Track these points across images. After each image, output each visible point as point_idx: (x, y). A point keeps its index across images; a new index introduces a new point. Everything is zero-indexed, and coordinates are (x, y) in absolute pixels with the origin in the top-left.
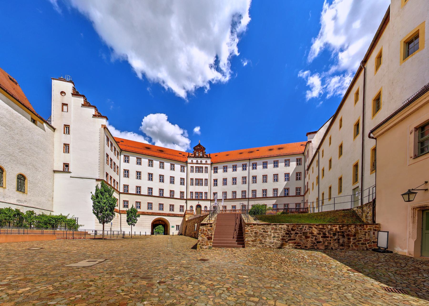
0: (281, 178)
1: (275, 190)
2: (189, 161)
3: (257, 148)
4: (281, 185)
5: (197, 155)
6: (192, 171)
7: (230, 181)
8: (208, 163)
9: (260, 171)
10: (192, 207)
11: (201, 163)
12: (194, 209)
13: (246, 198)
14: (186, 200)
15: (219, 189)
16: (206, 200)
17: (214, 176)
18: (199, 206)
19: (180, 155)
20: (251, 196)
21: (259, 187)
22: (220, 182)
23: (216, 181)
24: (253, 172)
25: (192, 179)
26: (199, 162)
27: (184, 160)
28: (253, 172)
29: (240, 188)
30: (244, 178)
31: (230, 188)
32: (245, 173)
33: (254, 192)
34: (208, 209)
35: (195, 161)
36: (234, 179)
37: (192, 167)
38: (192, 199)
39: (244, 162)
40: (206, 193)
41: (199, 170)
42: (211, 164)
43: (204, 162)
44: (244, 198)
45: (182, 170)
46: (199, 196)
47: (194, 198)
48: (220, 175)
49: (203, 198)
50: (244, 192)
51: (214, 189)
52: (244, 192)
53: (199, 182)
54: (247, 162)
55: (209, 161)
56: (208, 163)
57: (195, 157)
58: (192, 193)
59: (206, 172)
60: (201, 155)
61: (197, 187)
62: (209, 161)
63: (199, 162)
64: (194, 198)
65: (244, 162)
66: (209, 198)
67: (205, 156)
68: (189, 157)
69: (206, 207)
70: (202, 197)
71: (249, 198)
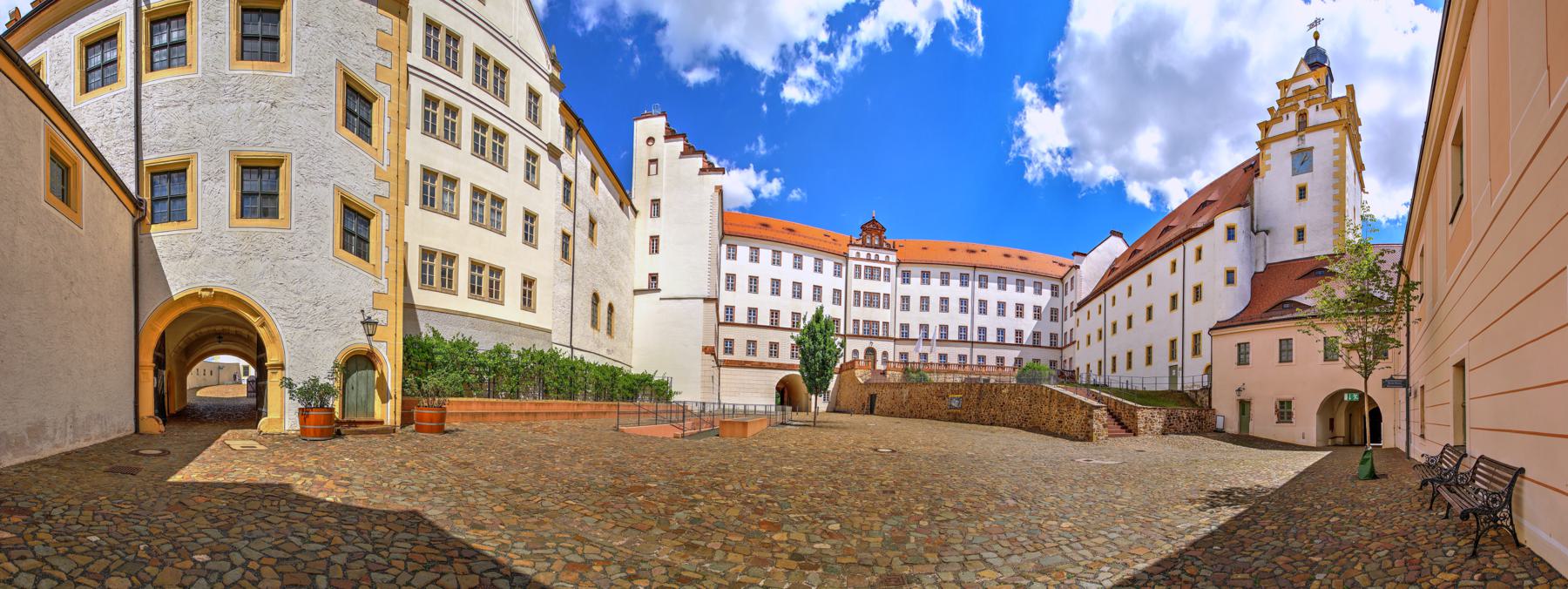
0: (1029, 312)
1: (1019, 333)
2: (852, 252)
3: (982, 246)
4: (1028, 325)
6: (858, 276)
7: (935, 304)
9: (992, 293)
10: (855, 352)
11: (877, 260)
12: (861, 356)
14: (845, 336)
15: (914, 318)
16: (887, 338)
17: (904, 289)
18: (871, 351)
20: (976, 338)
21: (991, 322)
22: (915, 303)
23: (906, 299)
24: (981, 294)
25: (857, 293)
27: (841, 250)
28: (981, 294)
29: (955, 320)
30: (963, 302)
32: (965, 292)
33: (983, 330)
34: (891, 358)
35: (863, 255)
36: (944, 300)
37: (858, 267)
38: (856, 336)
39: (965, 271)
40: (886, 324)
41: (872, 274)
42: (899, 263)
43: (882, 257)
44: (963, 340)
45: (837, 274)
48: (915, 288)
50: (963, 329)
51: (903, 317)
52: (963, 329)
53: (872, 300)
54: (970, 271)
55: (893, 258)
57: (864, 245)
58: (856, 321)
59: (887, 279)
62: (893, 258)
65: (965, 271)
66: (891, 335)
68: (851, 244)
69: (885, 354)
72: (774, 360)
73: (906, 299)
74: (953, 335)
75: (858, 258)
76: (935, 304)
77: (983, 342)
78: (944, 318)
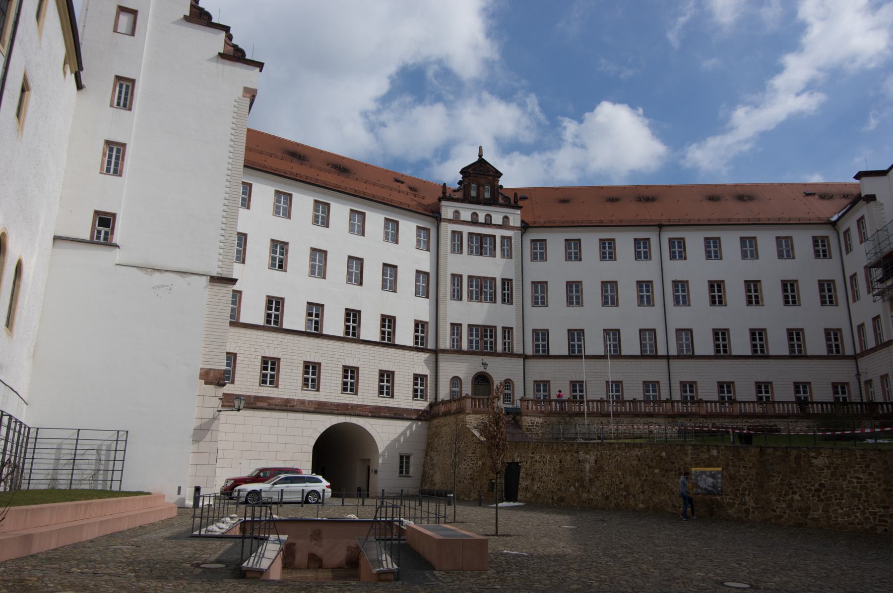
5: (473, 193)
6: (457, 248)
7: (592, 293)
8: (511, 224)
11: (488, 223)
13: (656, 357)
15: (557, 319)
16: (508, 353)
18: (482, 380)
19: (403, 187)
23: (540, 287)
25: (456, 278)
26: (481, 219)
29: (630, 318)
30: (645, 287)
31: (593, 318)
32: (647, 270)
35: (466, 215)
37: (457, 235)
38: (456, 351)
40: (507, 331)
41: (482, 245)
42: (525, 227)
43: (497, 219)
44: (648, 354)
46: (484, 339)
47: (465, 346)
49: (500, 348)
51: (537, 318)
54: (653, 236)
55: (515, 218)
56: (511, 224)
57: (466, 199)
58: (456, 327)
60: (487, 195)
61: (476, 305)
62: (515, 218)
63: (481, 219)
64: (465, 346)
67: (501, 201)
69: (508, 384)
70: (493, 344)
71: (668, 357)
72: (310, 396)
73: (540, 287)
74: (631, 345)
75: (456, 220)
76: (592, 293)
77: (688, 354)
78: (611, 317)
